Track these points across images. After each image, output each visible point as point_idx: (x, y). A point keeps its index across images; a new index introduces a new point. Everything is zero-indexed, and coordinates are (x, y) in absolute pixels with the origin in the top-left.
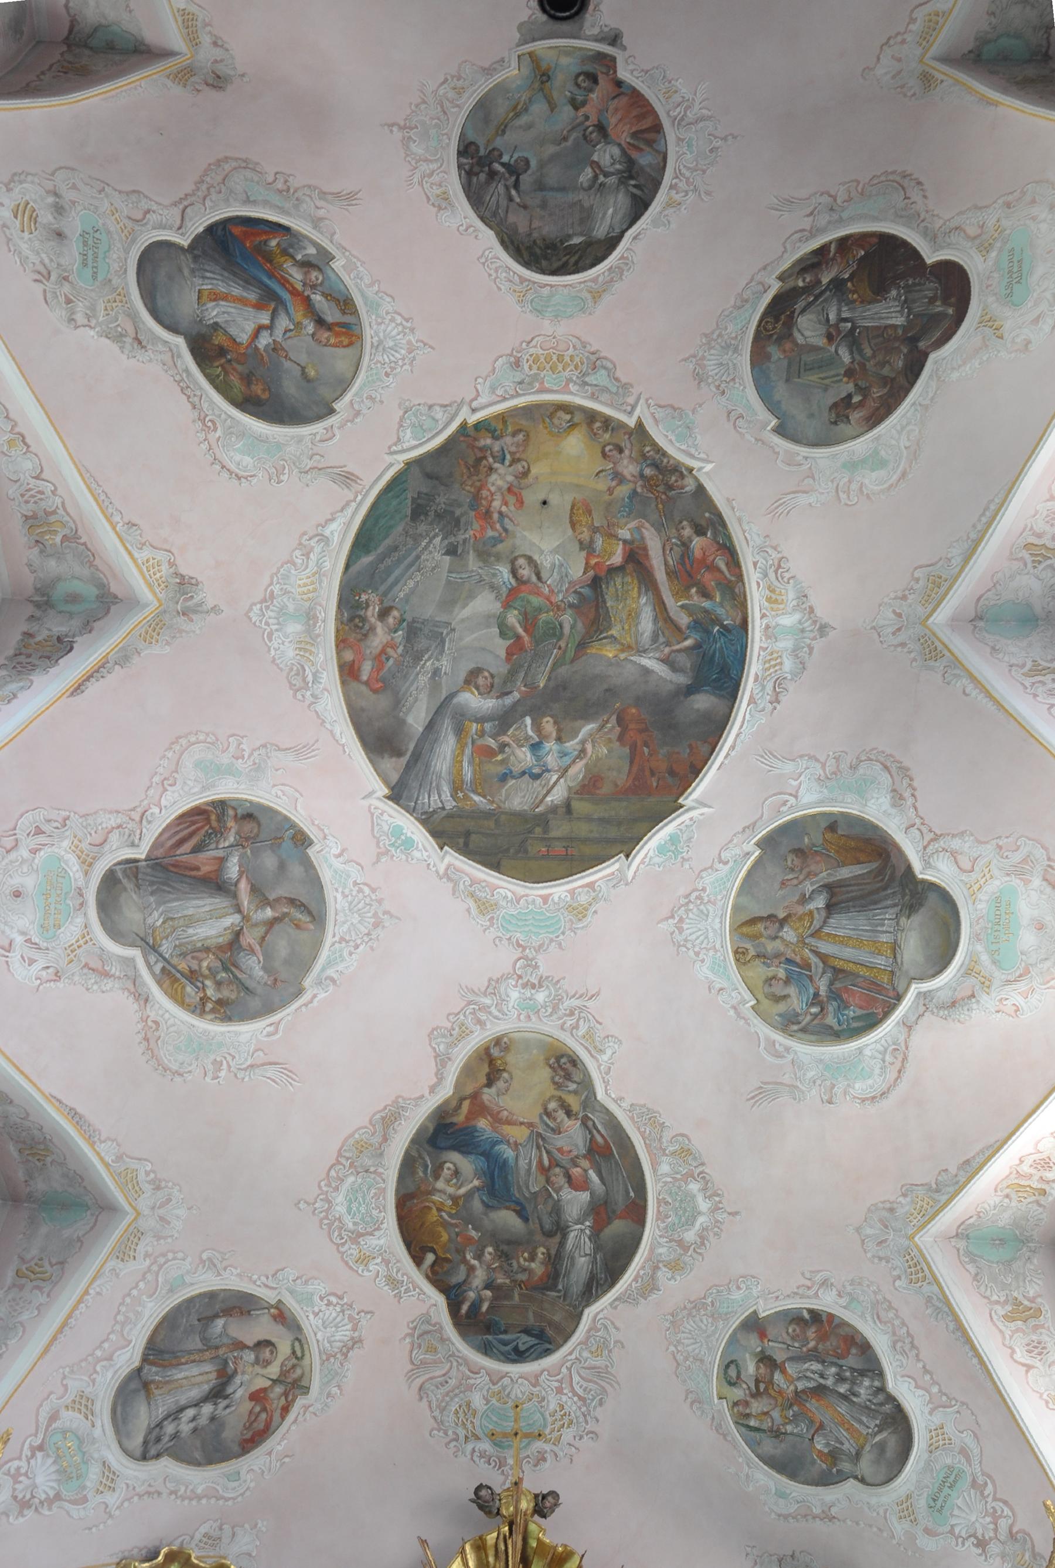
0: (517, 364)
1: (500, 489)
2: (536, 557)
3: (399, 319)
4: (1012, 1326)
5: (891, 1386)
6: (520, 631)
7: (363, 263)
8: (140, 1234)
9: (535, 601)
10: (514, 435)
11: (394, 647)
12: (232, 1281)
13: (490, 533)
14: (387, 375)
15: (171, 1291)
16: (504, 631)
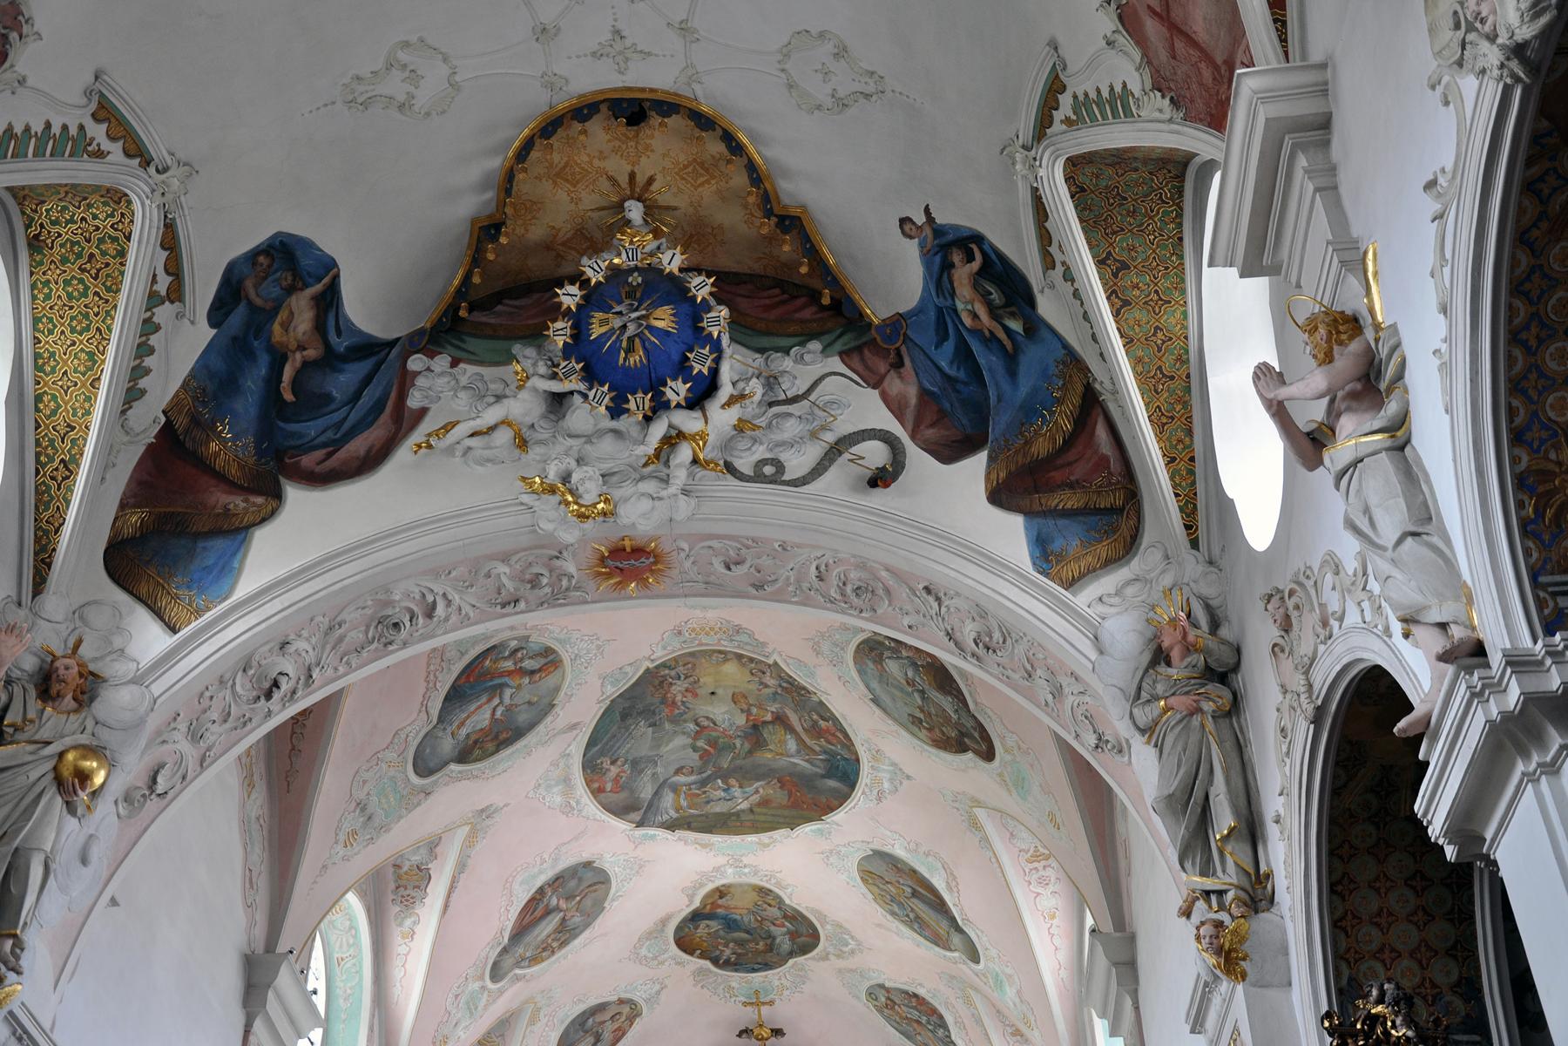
0: (680, 633)
1: (680, 691)
2: (711, 716)
3: (587, 638)
4: (1014, 1039)
5: (953, 1038)
6: (706, 747)
7: (551, 625)
8: (539, 1009)
9: (714, 734)
10: (684, 665)
11: (624, 772)
12: (593, 1001)
13: (677, 711)
14: (586, 668)
15: (562, 1022)
16: (695, 749)
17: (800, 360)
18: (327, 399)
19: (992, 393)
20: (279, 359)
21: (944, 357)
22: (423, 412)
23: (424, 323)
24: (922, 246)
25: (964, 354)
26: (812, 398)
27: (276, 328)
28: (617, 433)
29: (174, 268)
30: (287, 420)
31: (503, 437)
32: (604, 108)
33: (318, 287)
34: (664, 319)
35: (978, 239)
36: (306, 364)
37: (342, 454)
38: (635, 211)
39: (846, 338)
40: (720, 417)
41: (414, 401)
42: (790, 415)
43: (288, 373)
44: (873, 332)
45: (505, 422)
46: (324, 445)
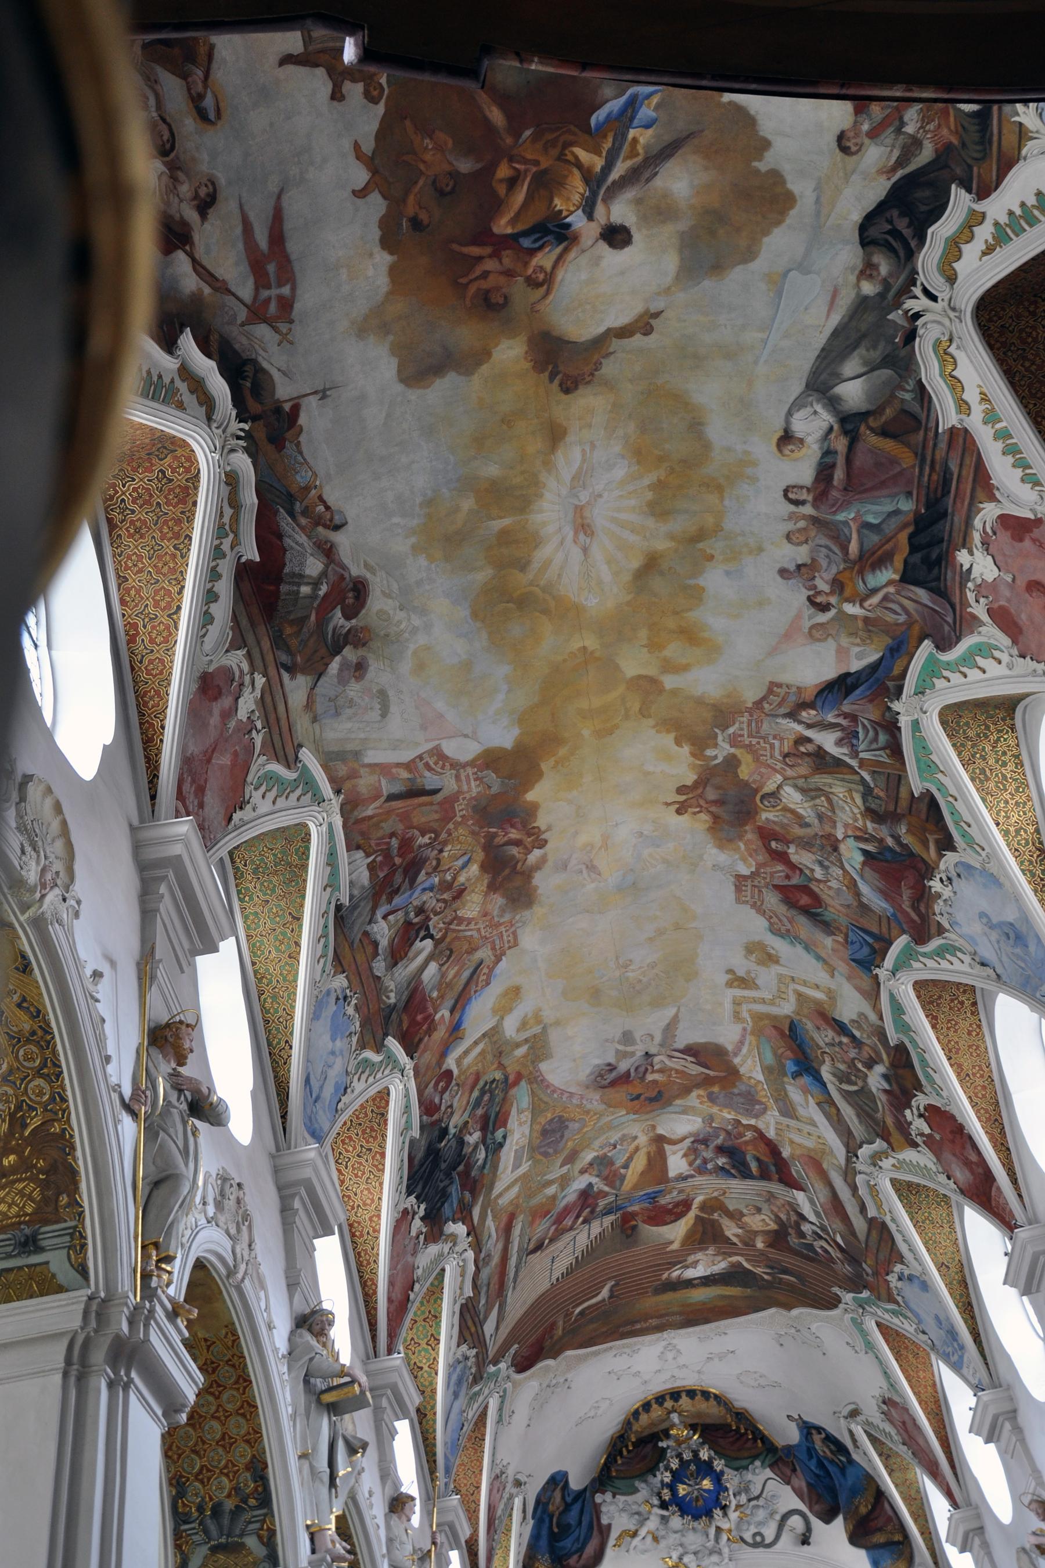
17: (754, 1473)
18: (569, 1526)
19: (836, 1482)
20: (551, 1517)
21: (813, 1464)
22: (609, 1526)
23: (594, 1475)
24: (798, 1425)
25: (821, 1464)
26: (764, 1495)
27: (550, 1506)
28: (693, 1529)
29: (524, 1511)
30: (557, 1541)
31: (649, 1538)
32: (668, 1397)
33: (562, 1484)
34: (707, 1484)
35: (824, 1429)
36: (560, 1514)
37: (584, 1556)
38: (675, 1418)
39: (770, 1456)
40: (734, 1516)
41: (605, 1521)
42: (757, 1507)
43: (555, 1520)
44: (780, 1453)
45: (648, 1532)
46: (576, 1552)
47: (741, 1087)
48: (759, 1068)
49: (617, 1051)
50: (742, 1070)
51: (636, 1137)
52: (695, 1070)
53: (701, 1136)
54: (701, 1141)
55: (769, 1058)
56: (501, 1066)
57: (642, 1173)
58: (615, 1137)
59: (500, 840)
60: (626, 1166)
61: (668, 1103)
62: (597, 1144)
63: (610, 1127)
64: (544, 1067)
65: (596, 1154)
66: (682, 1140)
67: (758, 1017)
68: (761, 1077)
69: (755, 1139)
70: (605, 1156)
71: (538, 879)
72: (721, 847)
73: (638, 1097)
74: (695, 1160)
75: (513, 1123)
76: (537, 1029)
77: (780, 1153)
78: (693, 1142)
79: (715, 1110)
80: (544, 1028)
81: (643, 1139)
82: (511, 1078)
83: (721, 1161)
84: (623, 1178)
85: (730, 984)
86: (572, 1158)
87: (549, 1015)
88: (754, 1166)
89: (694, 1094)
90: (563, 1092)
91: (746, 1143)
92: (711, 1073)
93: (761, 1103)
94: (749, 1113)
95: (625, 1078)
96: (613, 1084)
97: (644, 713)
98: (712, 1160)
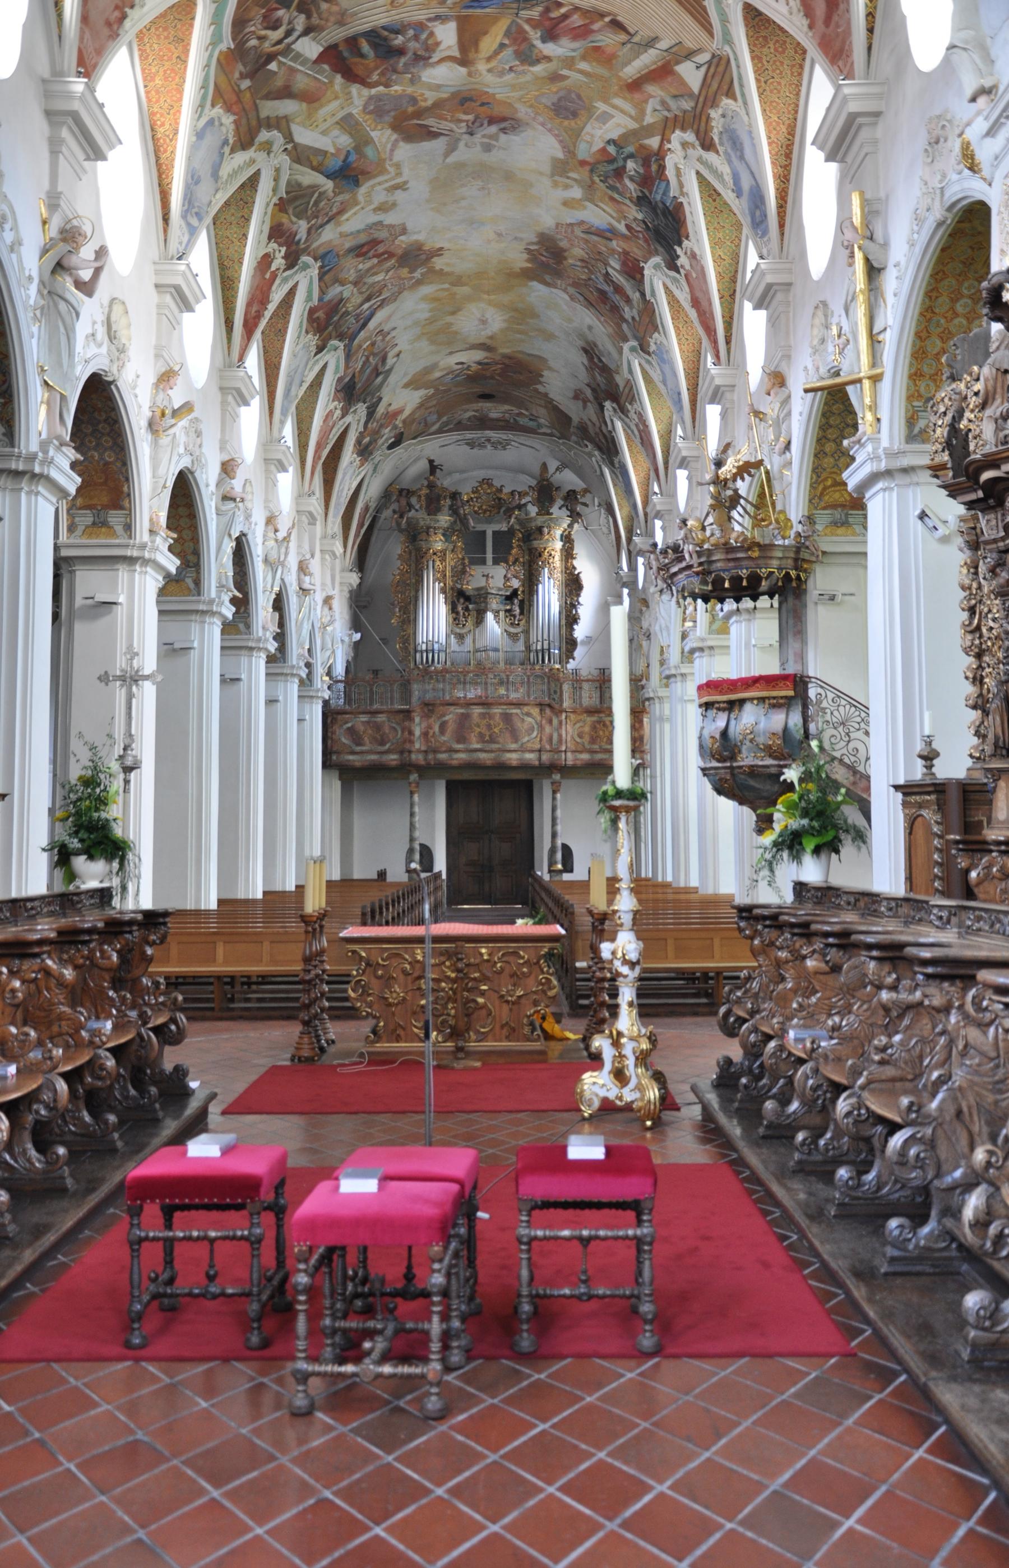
47: (388, 119)
48: (376, 139)
49: (497, 140)
50: (389, 131)
51: (489, 71)
52: (430, 122)
53: (421, 63)
54: (422, 59)
55: (369, 151)
56: (593, 182)
57: (485, 33)
58: (509, 77)
59: (551, 261)
60: (502, 46)
61: (454, 95)
62: (528, 77)
63: (513, 87)
64: (560, 155)
65: (532, 69)
66: (442, 60)
67: (383, 171)
68: (373, 134)
69: (368, 76)
70: (523, 62)
71: (535, 240)
72: (417, 241)
73: (483, 104)
74: (427, 39)
75: (598, 145)
76: (556, 178)
77: (343, 77)
78: (430, 58)
79: (410, 90)
80: (553, 175)
81: (482, 67)
82: (588, 168)
83: (399, 40)
84: (507, 34)
85: (406, 183)
86: (555, 78)
87: (547, 182)
88: (365, 47)
89: (429, 103)
90: (550, 130)
91: (376, 68)
92: (416, 121)
93: (370, 113)
94: (378, 98)
95: (492, 121)
96: (504, 119)
97: (460, 277)
98: (409, 40)
